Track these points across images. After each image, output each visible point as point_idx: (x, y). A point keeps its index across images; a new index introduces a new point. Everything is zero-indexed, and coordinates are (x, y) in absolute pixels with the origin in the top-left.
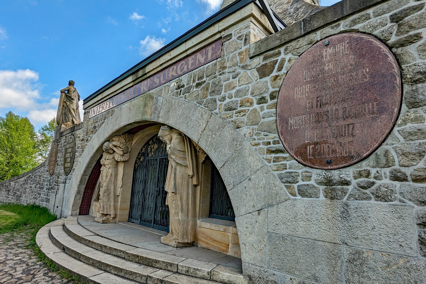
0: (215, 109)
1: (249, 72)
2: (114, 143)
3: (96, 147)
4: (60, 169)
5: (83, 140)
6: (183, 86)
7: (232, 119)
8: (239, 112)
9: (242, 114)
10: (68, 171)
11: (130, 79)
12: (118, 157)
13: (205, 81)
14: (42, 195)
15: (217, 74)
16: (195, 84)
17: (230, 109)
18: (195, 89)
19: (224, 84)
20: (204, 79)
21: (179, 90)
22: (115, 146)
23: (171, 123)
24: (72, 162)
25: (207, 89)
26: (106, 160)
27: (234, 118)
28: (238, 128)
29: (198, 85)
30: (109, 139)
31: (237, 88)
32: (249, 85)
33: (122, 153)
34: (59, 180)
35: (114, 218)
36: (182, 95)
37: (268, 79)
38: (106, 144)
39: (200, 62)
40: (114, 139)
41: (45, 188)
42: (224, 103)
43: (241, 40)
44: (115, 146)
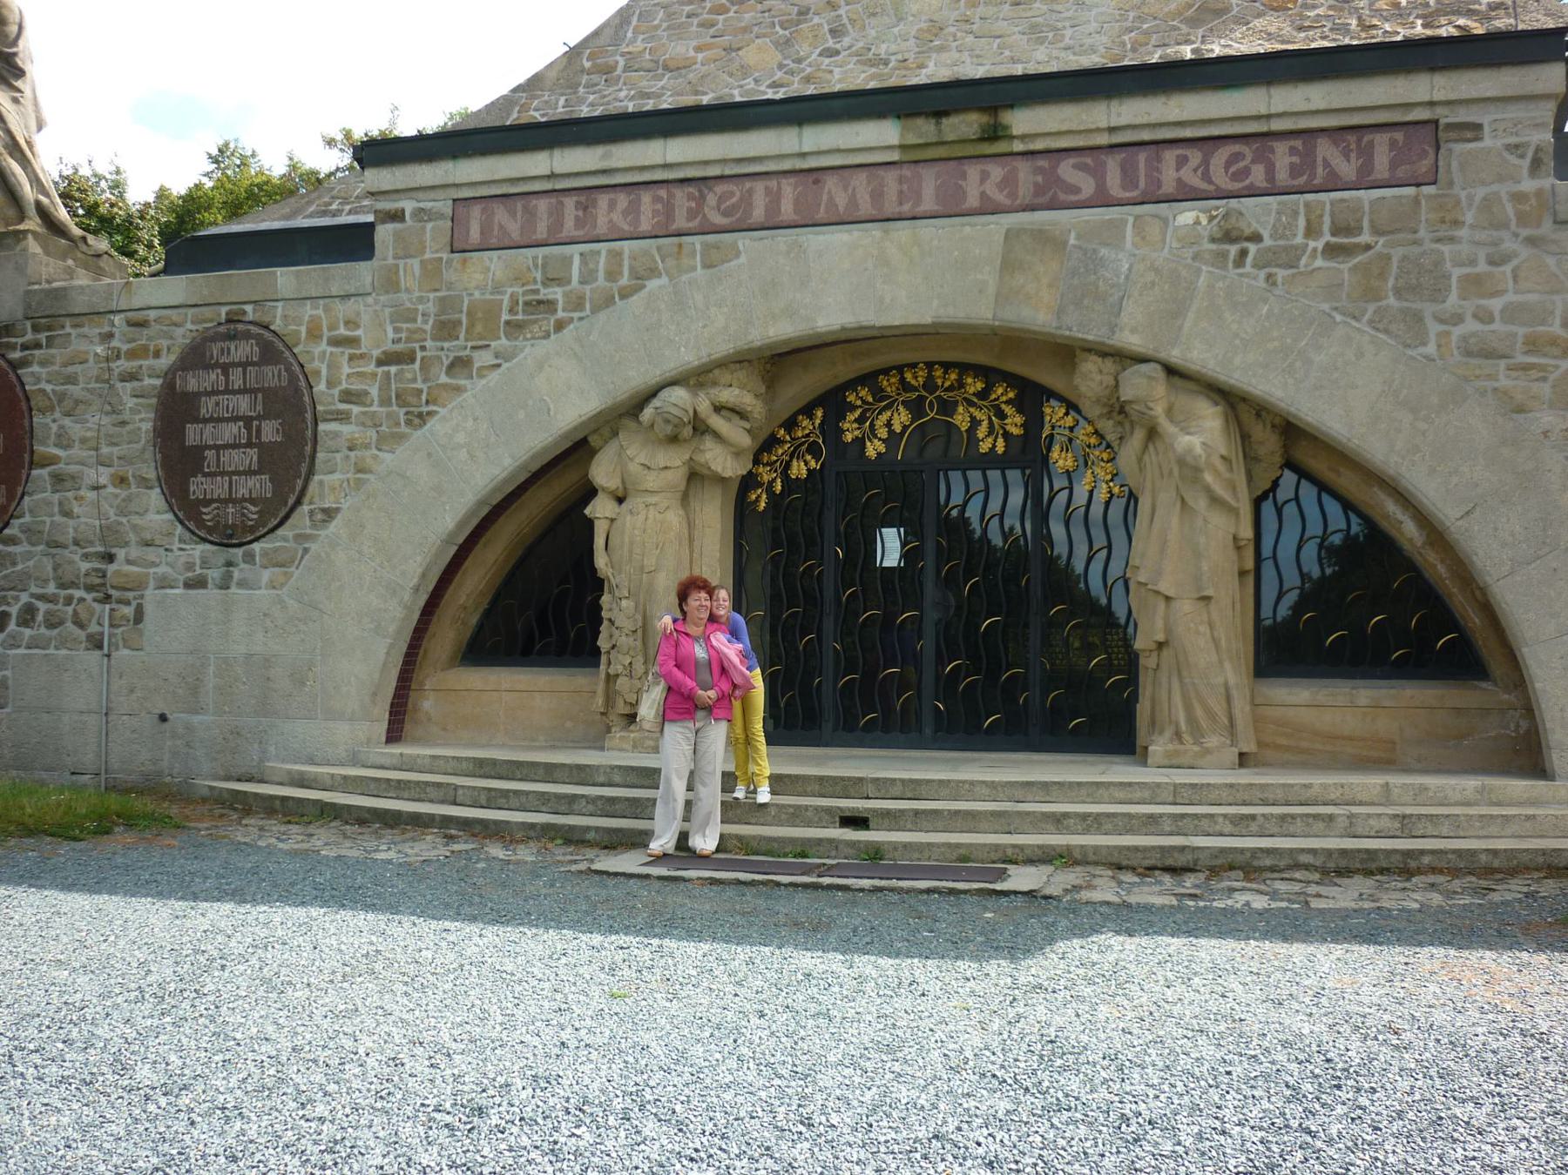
0: (1424, 344)
1: (1551, 261)
6: (1256, 238)
7: (1496, 385)
8: (1526, 368)
9: (1534, 374)
11: (881, 134)
13: (1368, 247)
15: (1422, 233)
16: (1320, 245)
17: (1490, 354)
18: (1319, 262)
19: (1457, 272)
20: (1365, 238)
21: (1233, 250)
23: (1198, 355)
25: (1383, 275)
27: (1504, 382)
28: (1520, 409)
31: (1510, 297)
32: (1555, 297)
36: (1248, 268)
38: (678, 395)
39: (1333, 174)
40: (725, 377)
42: (1457, 331)
43: (1522, 156)
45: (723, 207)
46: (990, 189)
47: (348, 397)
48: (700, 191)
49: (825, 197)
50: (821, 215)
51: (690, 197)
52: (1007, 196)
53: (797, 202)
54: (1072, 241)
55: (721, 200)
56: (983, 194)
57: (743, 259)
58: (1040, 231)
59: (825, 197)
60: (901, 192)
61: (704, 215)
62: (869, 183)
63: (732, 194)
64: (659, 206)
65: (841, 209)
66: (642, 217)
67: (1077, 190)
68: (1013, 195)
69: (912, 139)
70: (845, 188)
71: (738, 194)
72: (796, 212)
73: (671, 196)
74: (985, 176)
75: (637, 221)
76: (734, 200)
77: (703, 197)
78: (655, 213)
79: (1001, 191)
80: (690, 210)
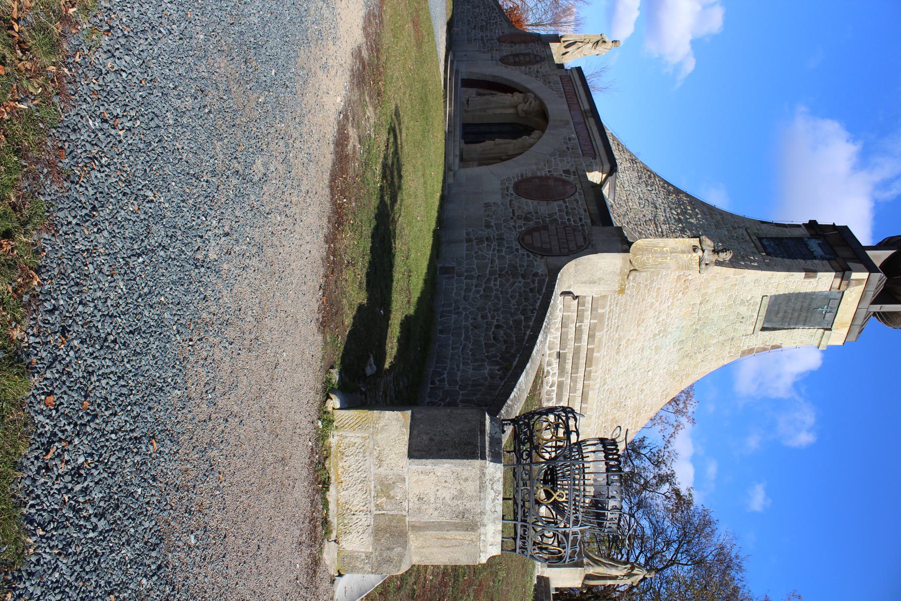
2: (533, 102)
3: (529, 86)
4: (507, 50)
5: (538, 72)
10: (504, 61)
11: (587, 106)
12: (520, 107)
14: (474, 31)
22: (530, 103)
24: (515, 64)
26: (517, 97)
29: (568, 148)
30: (536, 97)
33: (525, 109)
34: (495, 52)
35: (466, 111)
37: (562, 172)
40: (537, 102)
41: (481, 34)
44: (530, 103)
47: (530, 68)
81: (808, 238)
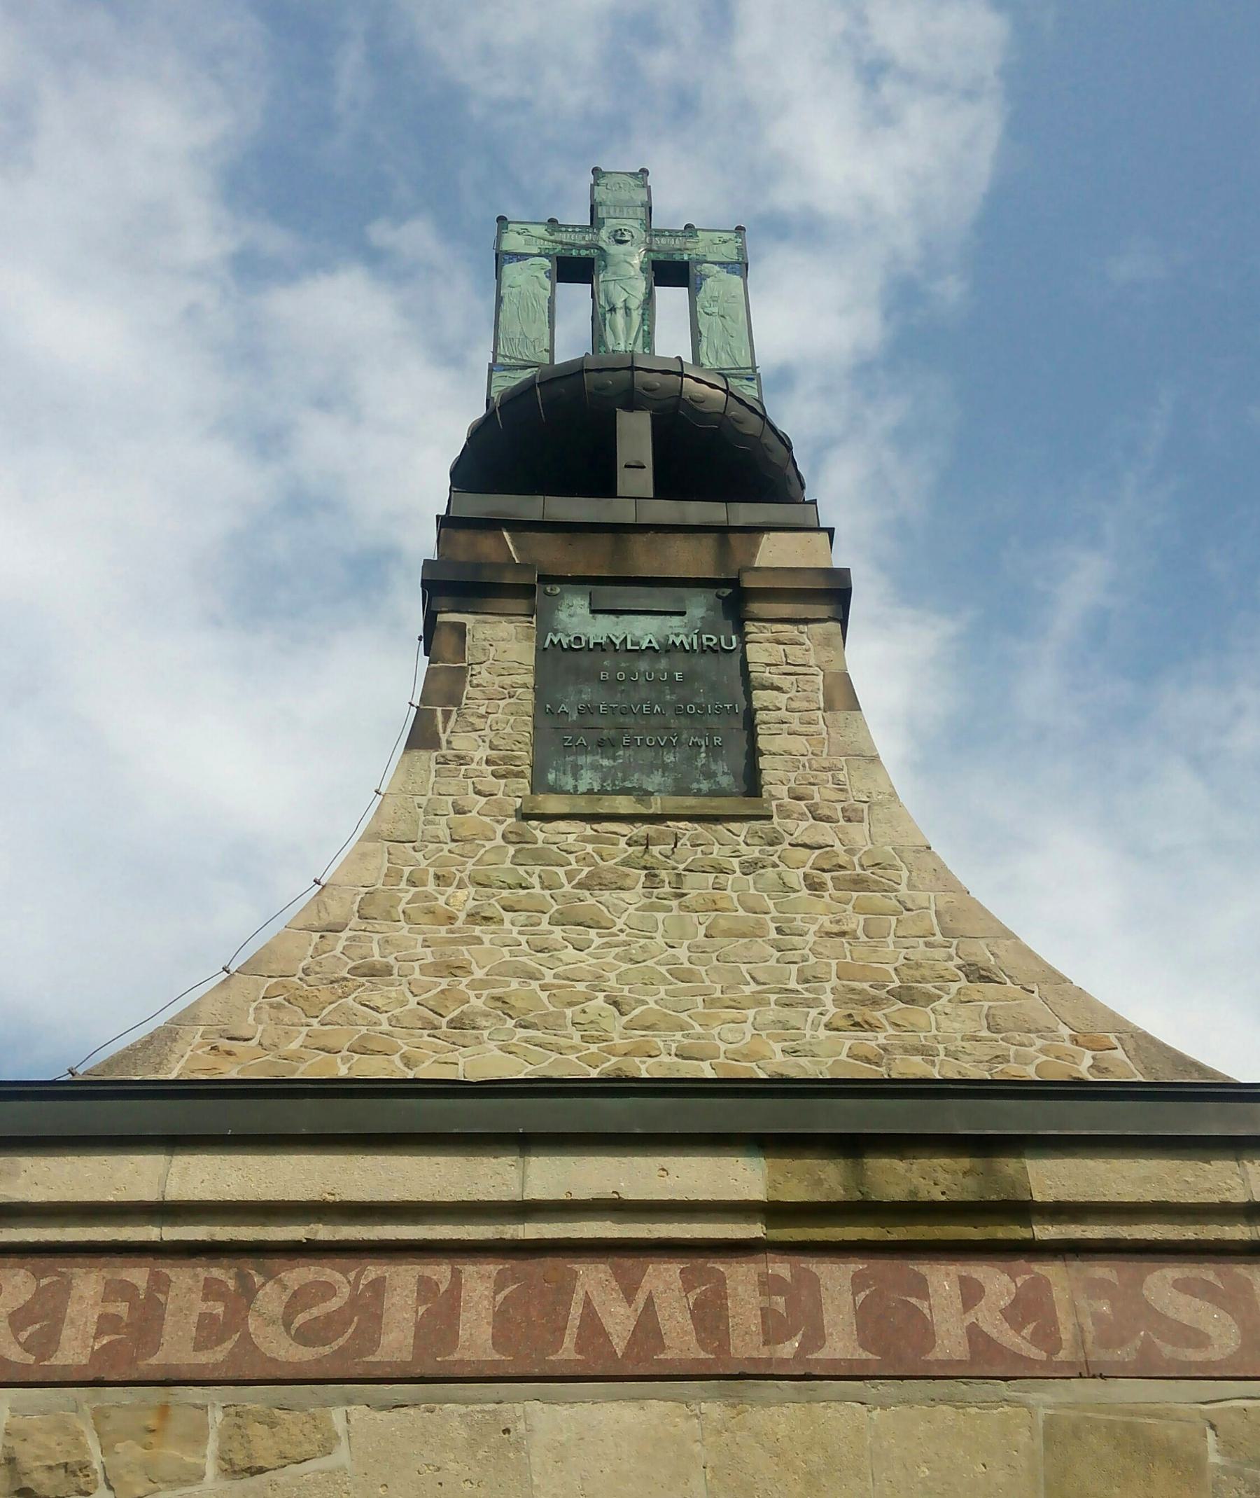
45: (300, 1319)
46: (989, 1319)
48: (242, 1278)
49: (576, 1311)
50: (568, 1352)
51: (211, 1290)
52: (1035, 1339)
53: (501, 1318)
54: (1214, 1458)
55: (298, 1301)
56: (974, 1334)
57: (342, 1455)
58: (1130, 1428)
59: (576, 1311)
60: (766, 1313)
61: (246, 1337)
62: (688, 1287)
63: (328, 1290)
64: (121, 1308)
65: (619, 1346)
66: (67, 1332)
67: (1198, 1339)
68: (1047, 1336)
69: (796, 1192)
70: (629, 1295)
71: (346, 1291)
72: (499, 1341)
73: (159, 1283)
74: (971, 1294)
75: (47, 1342)
76: (334, 1304)
77: (248, 1292)
78: (107, 1323)
79: (1018, 1327)
80: (206, 1321)
81: (543, 629)
